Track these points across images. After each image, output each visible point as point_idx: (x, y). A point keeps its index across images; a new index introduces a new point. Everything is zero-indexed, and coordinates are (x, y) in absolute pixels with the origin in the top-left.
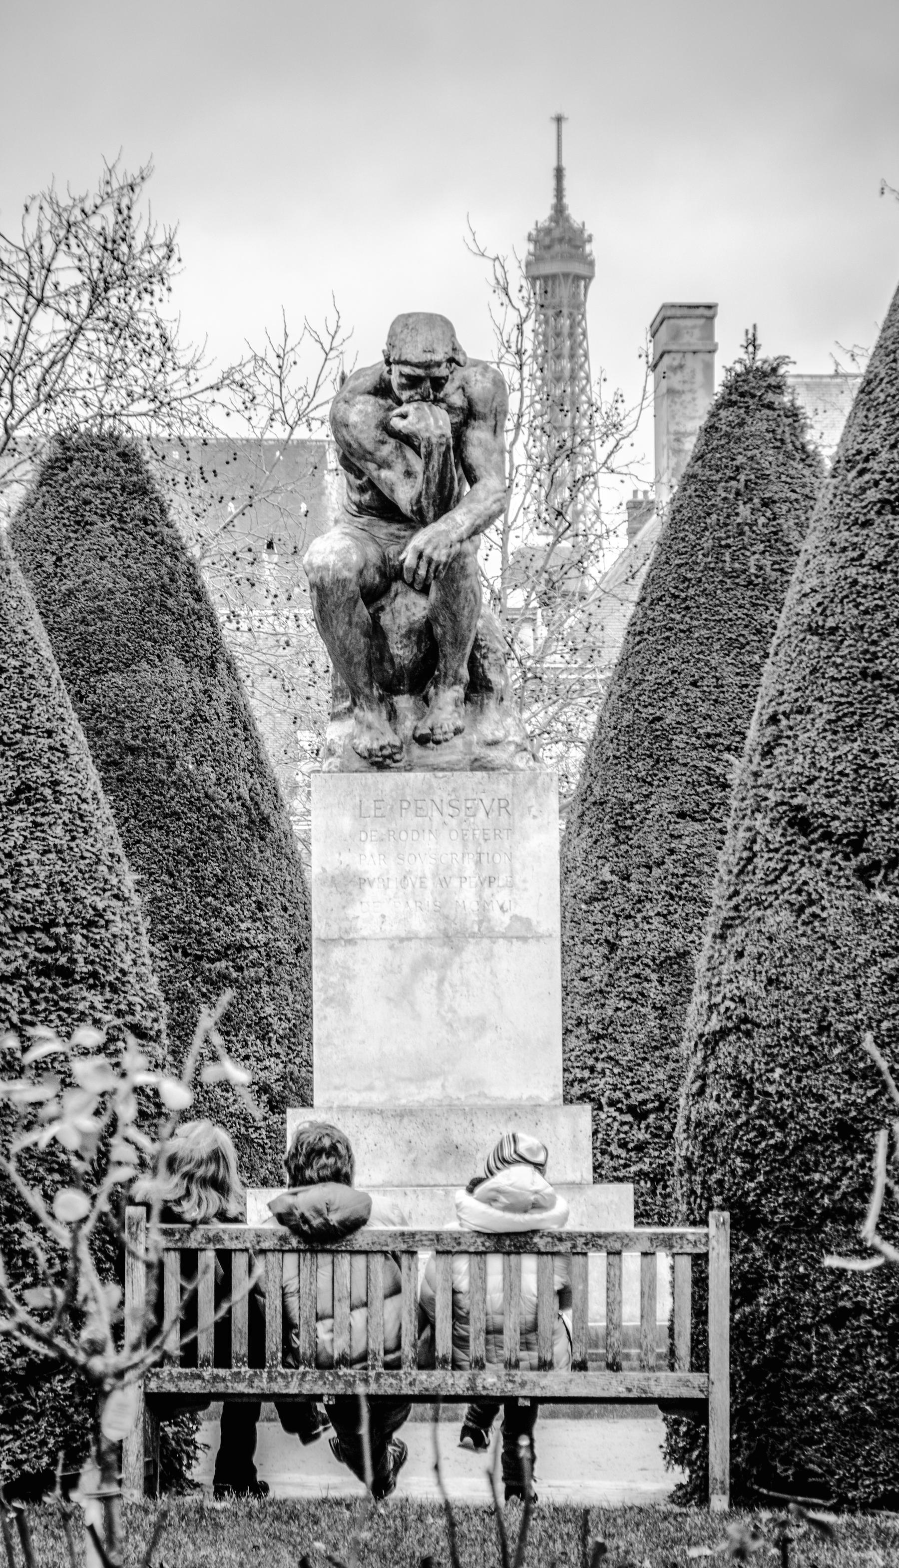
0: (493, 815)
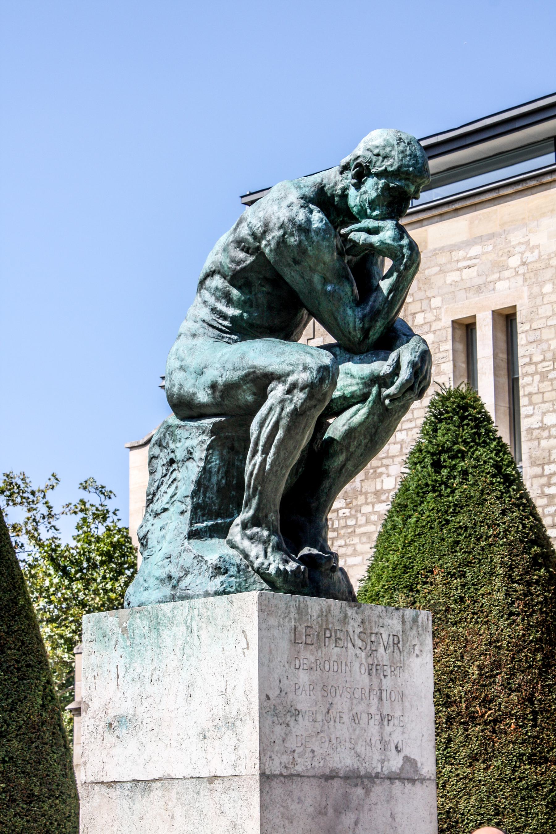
0: (389, 651)
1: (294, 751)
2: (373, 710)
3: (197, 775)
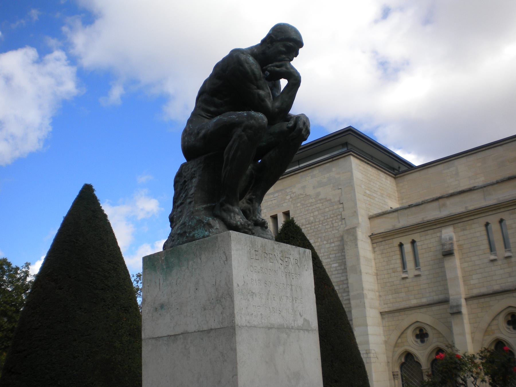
1: (252, 314)
2: (289, 295)
3: (201, 330)
